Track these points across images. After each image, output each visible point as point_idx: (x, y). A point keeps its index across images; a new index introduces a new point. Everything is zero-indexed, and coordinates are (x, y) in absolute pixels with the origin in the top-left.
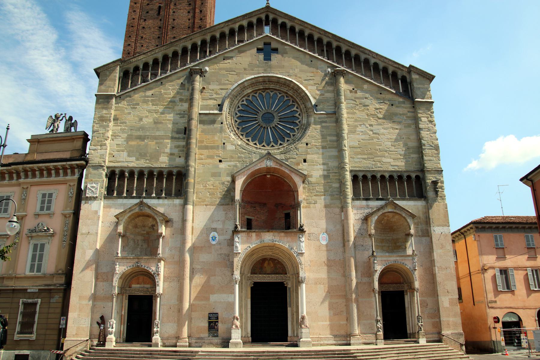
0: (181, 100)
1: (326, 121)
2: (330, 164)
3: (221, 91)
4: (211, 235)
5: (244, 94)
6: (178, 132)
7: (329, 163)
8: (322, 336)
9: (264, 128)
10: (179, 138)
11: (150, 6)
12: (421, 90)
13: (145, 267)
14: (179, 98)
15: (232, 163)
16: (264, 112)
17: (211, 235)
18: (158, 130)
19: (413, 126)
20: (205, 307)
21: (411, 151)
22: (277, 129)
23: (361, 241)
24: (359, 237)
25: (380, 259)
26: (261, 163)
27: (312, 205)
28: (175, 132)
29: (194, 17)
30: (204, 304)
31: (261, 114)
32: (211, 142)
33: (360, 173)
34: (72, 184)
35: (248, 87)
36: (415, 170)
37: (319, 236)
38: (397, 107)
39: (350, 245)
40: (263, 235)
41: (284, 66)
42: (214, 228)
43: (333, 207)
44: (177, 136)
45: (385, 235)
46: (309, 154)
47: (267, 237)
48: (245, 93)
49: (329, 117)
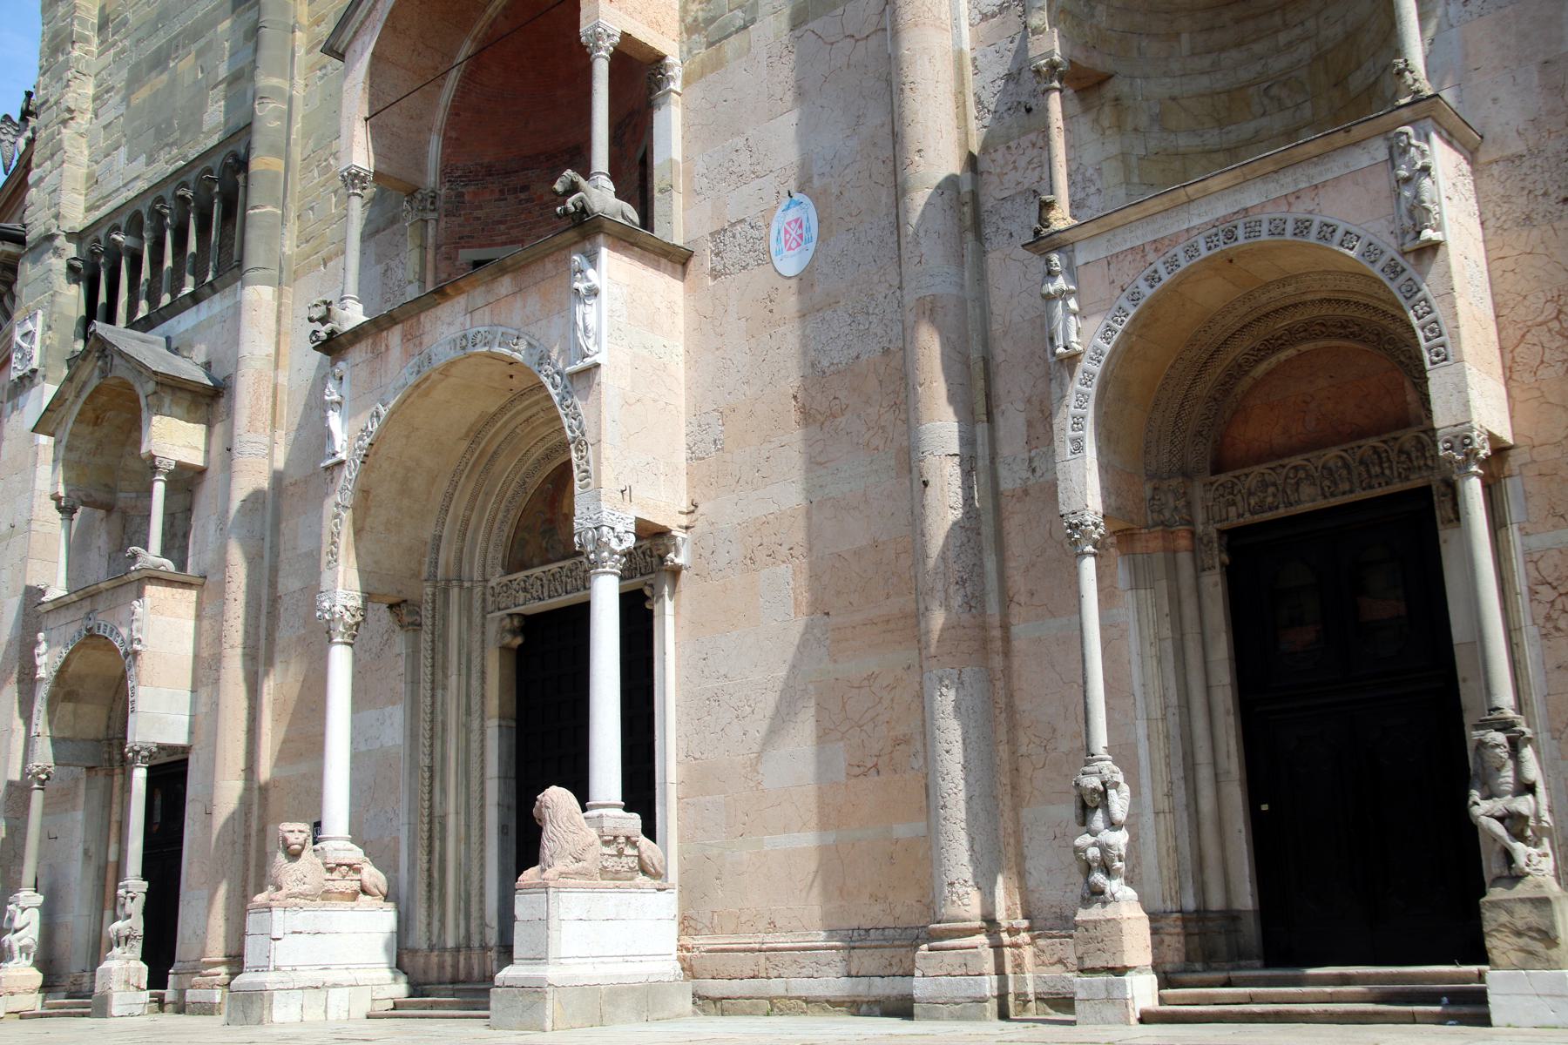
8: (783, 941)
23: (1022, 163)
24: (1010, 139)
25: (1101, 250)
39: (914, 218)
45: (1258, 48)
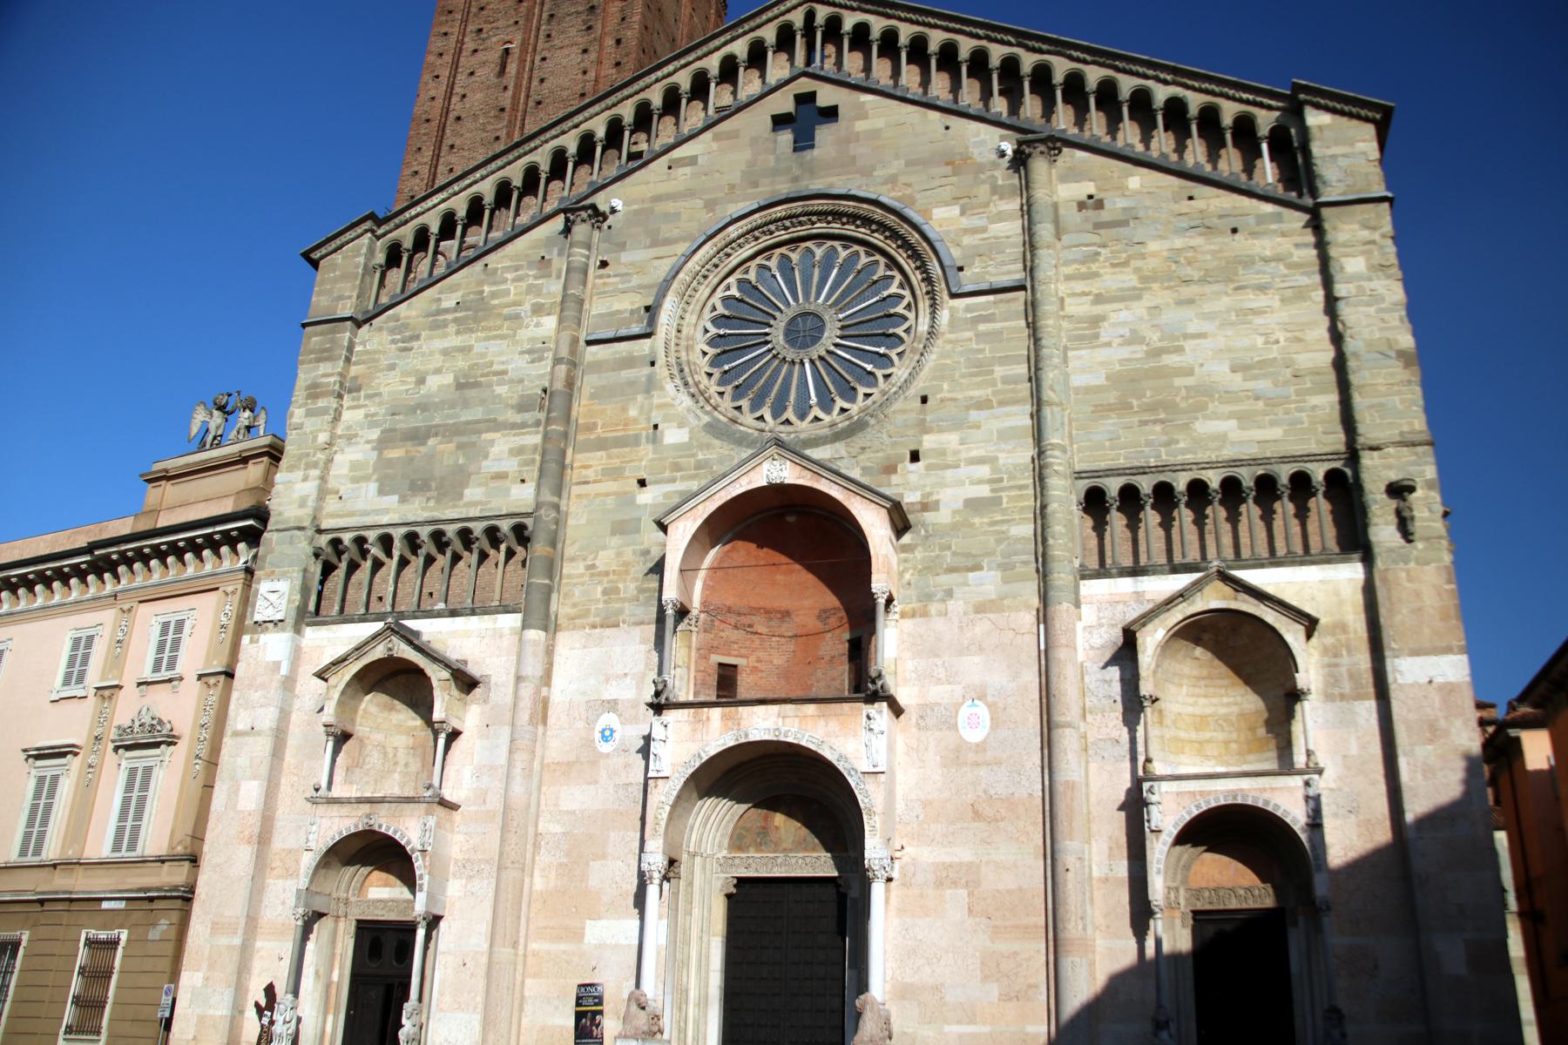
0: (538, 310)
1: (993, 314)
2: (1003, 459)
3: (657, 263)
4: (599, 727)
5: (731, 266)
6: (522, 407)
7: (1000, 455)
9: (793, 362)
10: (523, 425)
11: (480, 56)
12: (1342, 162)
13: (388, 828)
14: (533, 305)
16: (790, 313)
17: (599, 727)
18: (466, 404)
20: (568, 962)
21: (1309, 385)
22: (832, 362)
23: (1111, 725)
26: (751, 474)
27: (934, 608)
28: (512, 407)
30: (564, 952)
31: (780, 325)
32: (617, 425)
33: (1112, 479)
34: (230, 589)
35: (742, 240)
36: (1328, 449)
37: (957, 712)
38: (1254, 234)
40: (745, 715)
41: (854, 158)
42: (609, 702)
43: (1009, 607)
45: (1214, 700)
46: (927, 431)
47: (760, 720)
48: (734, 261)
49: (1001, 301)
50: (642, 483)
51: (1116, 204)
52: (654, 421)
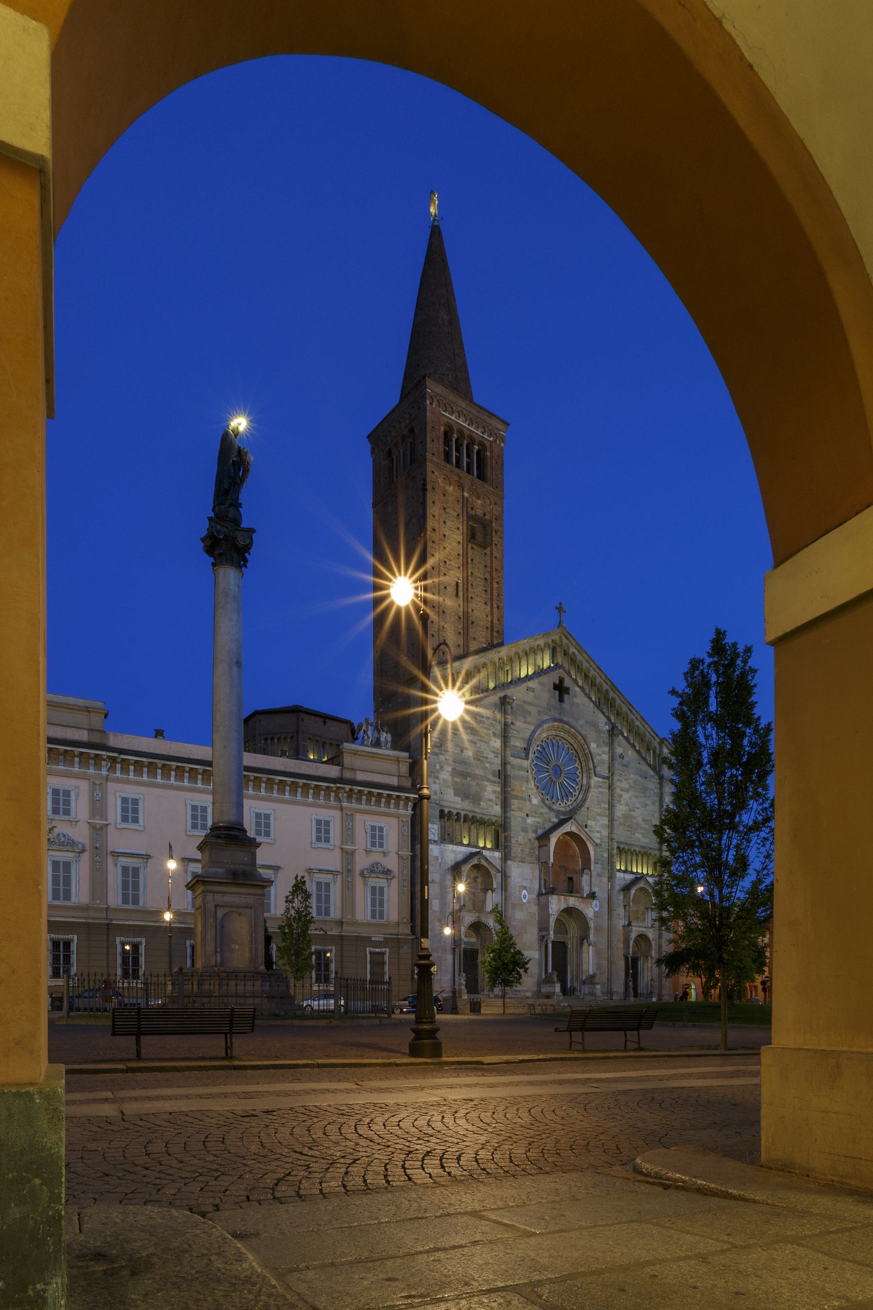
0: (494, 734)
6: (494, 775)
15: (537, 819)
19: (657, 804)
29: (492, 613)
31: (553, 764)
44: (493, 778)
50: (527, 815)
51: (626, 759)
52: (530, 794)
